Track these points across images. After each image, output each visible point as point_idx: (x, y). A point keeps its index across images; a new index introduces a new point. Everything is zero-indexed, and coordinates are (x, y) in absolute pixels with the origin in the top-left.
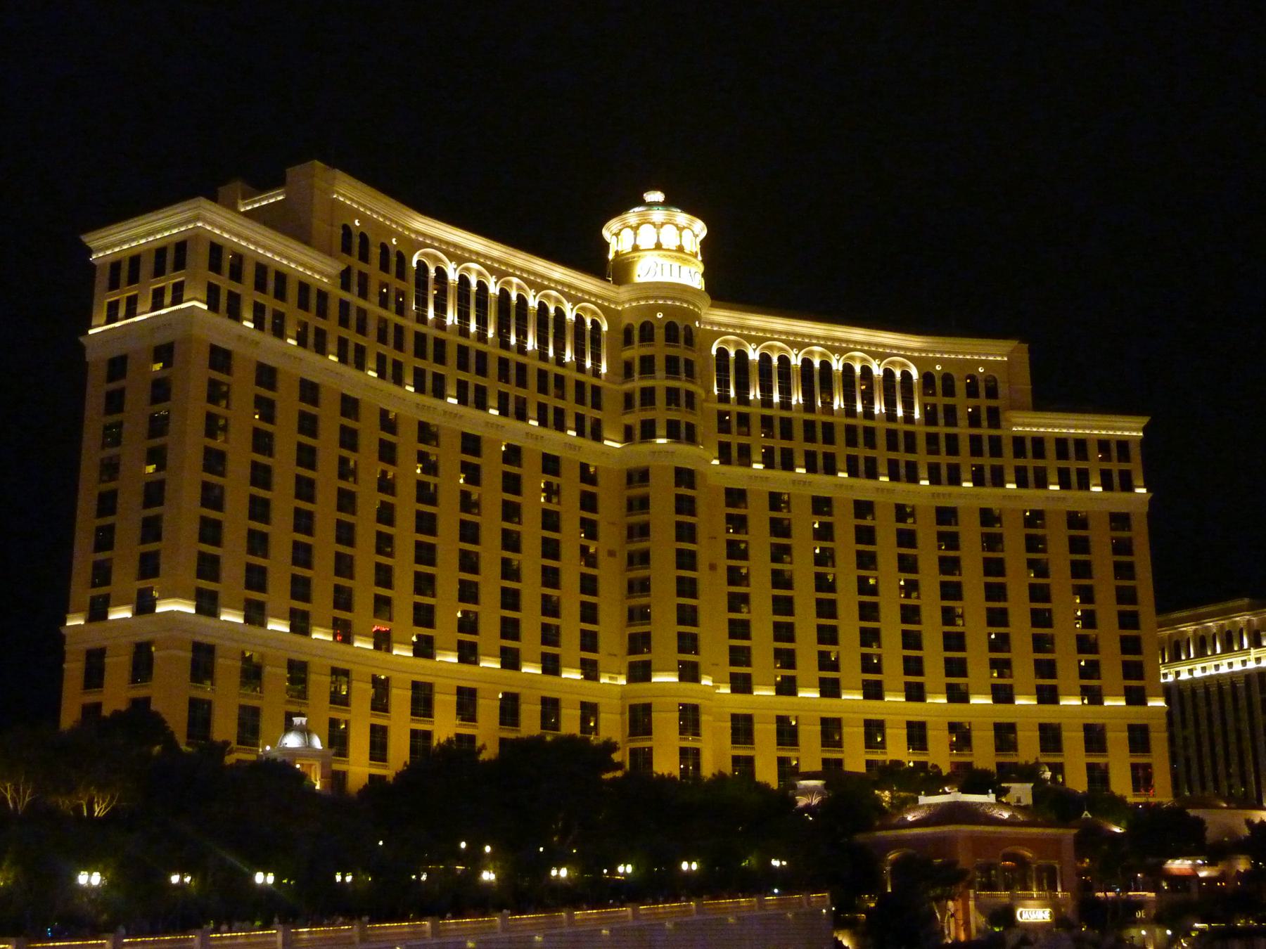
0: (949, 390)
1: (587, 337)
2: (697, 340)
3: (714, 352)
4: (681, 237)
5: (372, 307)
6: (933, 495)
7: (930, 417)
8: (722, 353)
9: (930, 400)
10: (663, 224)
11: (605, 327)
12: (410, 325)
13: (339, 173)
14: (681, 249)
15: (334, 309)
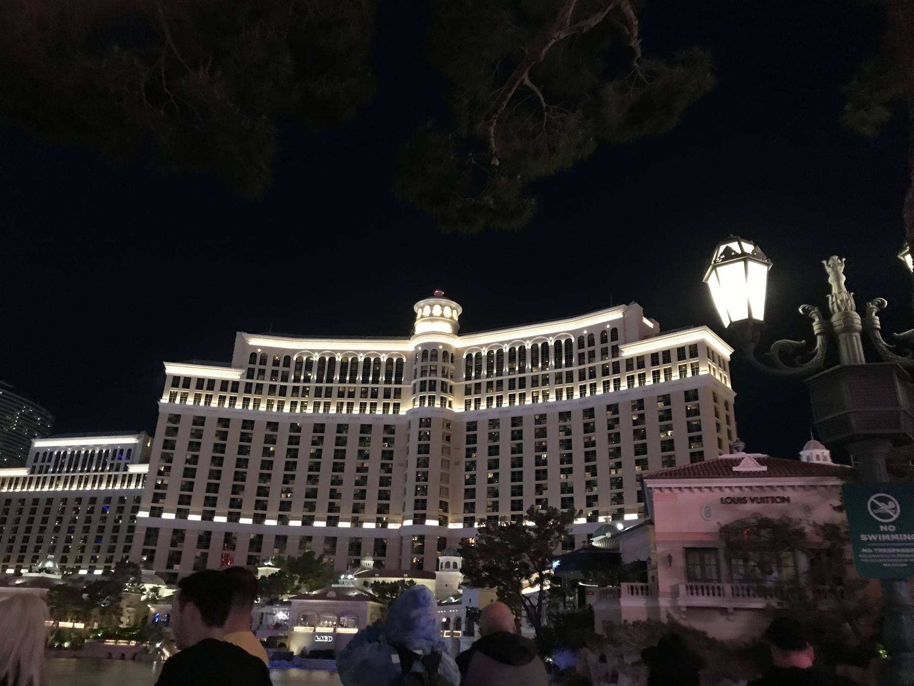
0: (591, 343)
1: (396, 368)
2: (440, 356)
3: (464, 356)
4: (432, 309)
5: (267, 382)
6: (579, 403)
7: (581, 361)
8: (469, 356)
9: (581, 351)
10: (424, 306)
11: (405, 360)
12: (290, 385)
13: (245, 335)
14: (431, 315)
15: (242, 388)
